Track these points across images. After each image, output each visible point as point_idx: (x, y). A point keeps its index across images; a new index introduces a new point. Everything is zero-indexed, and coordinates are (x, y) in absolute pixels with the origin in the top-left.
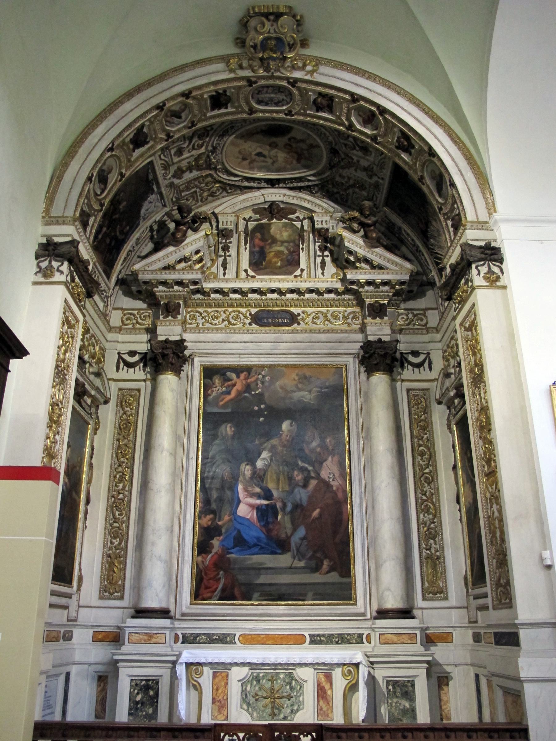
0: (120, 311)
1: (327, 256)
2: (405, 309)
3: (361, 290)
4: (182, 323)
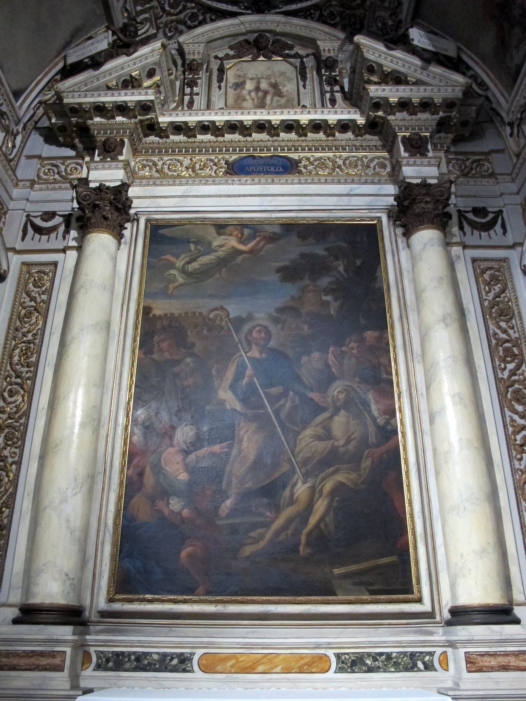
0: (36, 160)
1: (337, 92)
2: (456, 153)
3: (390, 118)
4: (125, 165)
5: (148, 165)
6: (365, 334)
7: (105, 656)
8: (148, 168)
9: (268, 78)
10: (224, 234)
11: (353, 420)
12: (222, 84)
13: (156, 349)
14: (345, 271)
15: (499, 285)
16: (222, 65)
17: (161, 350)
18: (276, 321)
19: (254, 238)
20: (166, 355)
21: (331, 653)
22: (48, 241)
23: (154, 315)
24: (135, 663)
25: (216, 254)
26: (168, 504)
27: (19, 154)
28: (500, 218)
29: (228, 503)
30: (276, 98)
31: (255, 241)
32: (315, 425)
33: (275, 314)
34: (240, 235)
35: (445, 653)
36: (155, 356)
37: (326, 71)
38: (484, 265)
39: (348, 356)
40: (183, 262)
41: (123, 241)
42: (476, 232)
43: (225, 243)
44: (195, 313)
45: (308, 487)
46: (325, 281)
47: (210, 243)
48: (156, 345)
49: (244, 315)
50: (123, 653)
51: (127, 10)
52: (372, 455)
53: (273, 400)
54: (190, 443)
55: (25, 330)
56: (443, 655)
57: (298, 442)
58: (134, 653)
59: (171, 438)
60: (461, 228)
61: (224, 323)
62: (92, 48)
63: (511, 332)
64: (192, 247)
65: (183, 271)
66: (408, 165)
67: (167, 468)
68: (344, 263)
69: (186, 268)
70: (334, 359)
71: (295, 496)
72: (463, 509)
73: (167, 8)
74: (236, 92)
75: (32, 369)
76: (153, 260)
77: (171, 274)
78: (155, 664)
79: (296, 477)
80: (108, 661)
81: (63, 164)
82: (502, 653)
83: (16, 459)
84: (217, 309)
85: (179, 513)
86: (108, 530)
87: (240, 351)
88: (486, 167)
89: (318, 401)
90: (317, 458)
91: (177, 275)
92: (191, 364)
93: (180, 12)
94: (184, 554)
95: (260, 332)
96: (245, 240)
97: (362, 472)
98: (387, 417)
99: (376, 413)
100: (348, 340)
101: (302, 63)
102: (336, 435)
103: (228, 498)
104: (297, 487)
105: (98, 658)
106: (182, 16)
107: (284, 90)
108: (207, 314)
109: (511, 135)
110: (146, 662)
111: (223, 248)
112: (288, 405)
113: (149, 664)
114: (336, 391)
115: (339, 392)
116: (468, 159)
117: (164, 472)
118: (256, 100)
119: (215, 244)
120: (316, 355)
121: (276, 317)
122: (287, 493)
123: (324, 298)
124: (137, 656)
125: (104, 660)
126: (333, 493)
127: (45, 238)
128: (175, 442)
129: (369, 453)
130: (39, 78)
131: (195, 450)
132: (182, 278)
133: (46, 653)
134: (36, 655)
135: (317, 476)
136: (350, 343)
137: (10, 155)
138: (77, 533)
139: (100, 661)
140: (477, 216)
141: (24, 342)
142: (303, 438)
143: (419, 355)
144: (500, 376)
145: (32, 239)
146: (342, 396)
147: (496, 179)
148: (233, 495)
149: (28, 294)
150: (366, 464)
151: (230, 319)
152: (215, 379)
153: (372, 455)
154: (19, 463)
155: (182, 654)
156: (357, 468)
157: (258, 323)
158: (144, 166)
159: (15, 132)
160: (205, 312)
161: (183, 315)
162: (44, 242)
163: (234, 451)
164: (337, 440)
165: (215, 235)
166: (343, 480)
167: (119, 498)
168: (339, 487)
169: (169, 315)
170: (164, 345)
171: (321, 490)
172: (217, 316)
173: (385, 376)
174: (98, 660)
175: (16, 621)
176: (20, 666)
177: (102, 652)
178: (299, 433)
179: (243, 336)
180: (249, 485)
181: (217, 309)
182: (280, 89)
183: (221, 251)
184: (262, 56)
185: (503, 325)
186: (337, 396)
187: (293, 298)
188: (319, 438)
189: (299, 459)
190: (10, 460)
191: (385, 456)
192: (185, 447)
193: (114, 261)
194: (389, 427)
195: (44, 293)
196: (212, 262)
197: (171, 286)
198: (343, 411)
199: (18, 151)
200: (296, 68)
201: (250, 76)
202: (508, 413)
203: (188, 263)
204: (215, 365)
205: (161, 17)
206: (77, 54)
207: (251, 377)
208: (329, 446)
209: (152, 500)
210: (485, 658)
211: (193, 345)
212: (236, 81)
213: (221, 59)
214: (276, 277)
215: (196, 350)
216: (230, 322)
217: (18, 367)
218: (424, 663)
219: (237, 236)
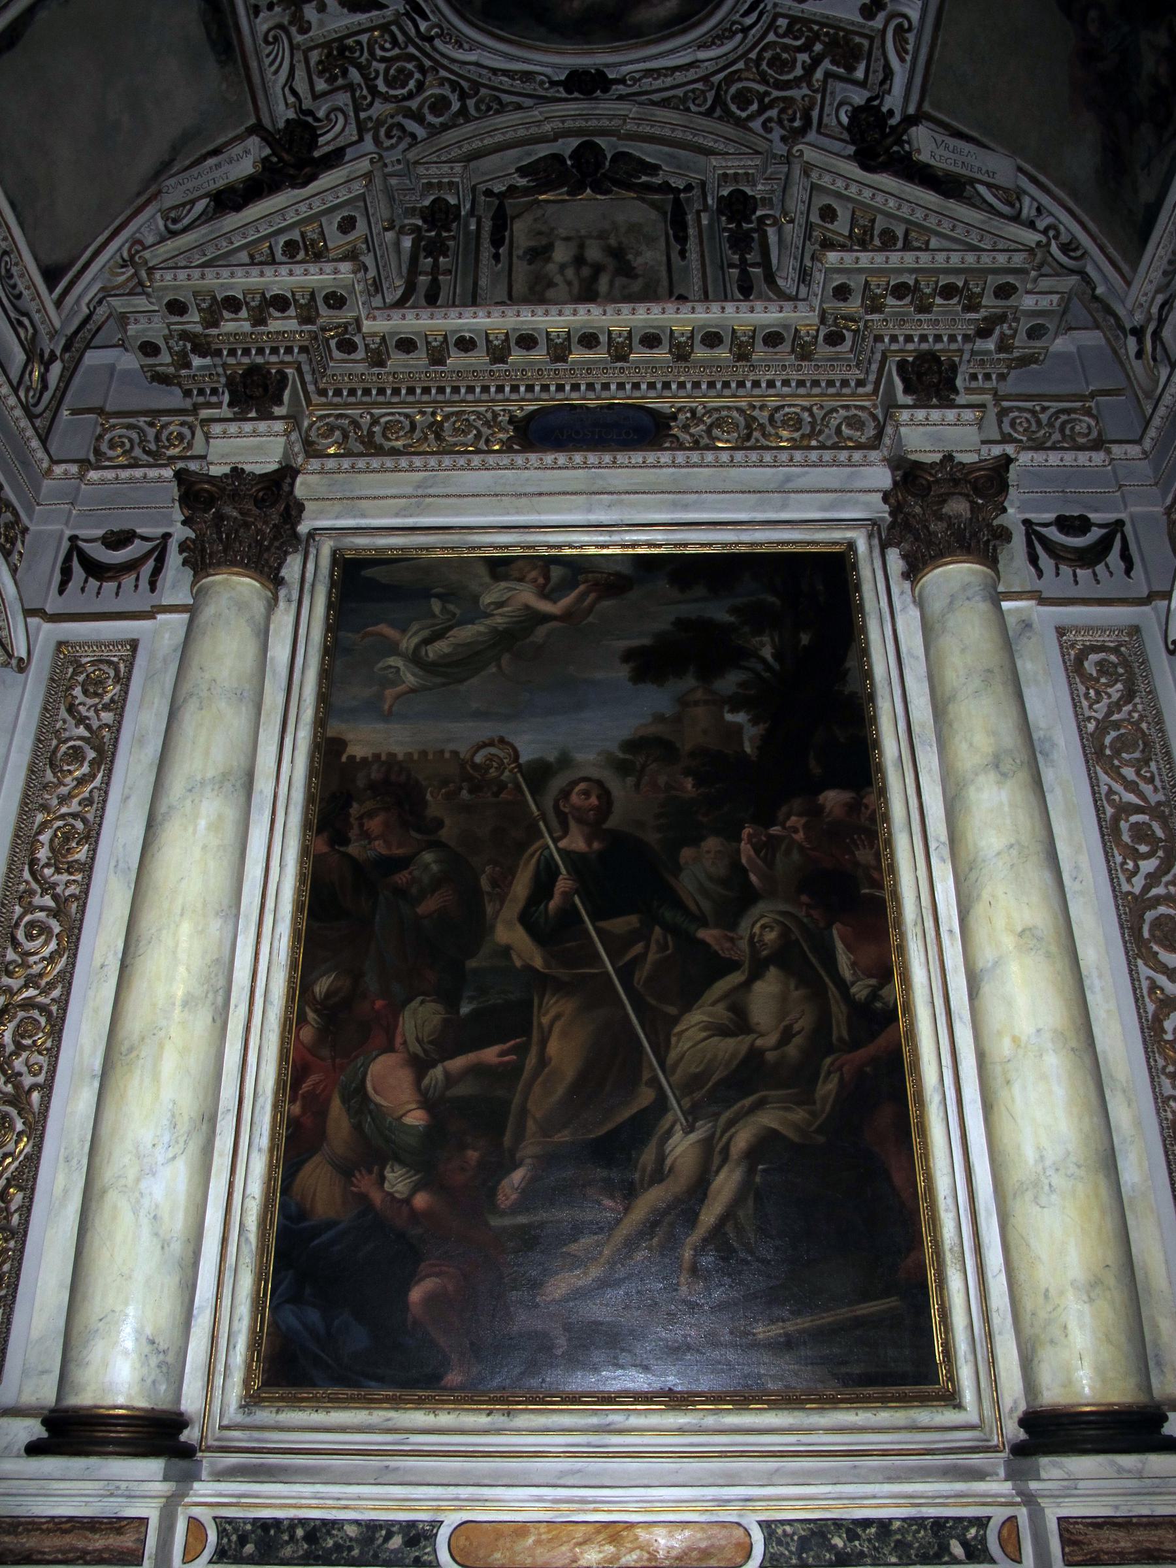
1: (753, 265)
5: (338, 427)
6: (821, 798)
7: (236, 1530)
8: (337, 433)
9: (602, 236)
10: (506, 578)
11: (797, 989)
12: (501, 251)
13: (353, 834)
14: (776, 656)
15: (1119, 686)
16: (501, 209)
17: (366, 835)
18: (622, 768)
19: (575, 586)
20: (379, 847)
21: (751, 1521)
22: (117, 594)
23: (352, 758)
24: (306, 1546)
25: (488, 622)
26: (382, 1179)
28: (1119, 536)
29: (518, 1176)
30: (620, 281)
31: (574, 594)
32: (710, 1002)
33: (621, 755)
34: (541, 581)
35: (1012, 1519)
36: (353, 849)
37: (729, 221)
38: (1083, 639)
39: (783, 847)
40: (416, 640)
41: (282, 593)
42: (1065, 569)
43: (509, 599)
44: (442, 752)
45: (698, 1141)
46: (729, 682)
47: (476, 599)
49: (551, 757)
50: (277, 1522)
51: (294, 93)
52: (840, 1069)
53: (616, 948)
54: (430, 1042)
55: (64, 790)
56: (1008, 1524)
57: (674, 1040)
58: (303, 1522)
59: (390, 1031)
60: (1033, 560)
61: (507, 773)
62: (217, 174)
63: (1147, 789)
64: (436, 606)
65: (416, 659)
66: (912, 422)
67: (378, 1099)
68: (773, 640)
69: (423, 653)
70: (752, 853)
71: (668, 1162)
72: (1047, 1188)
73: (382, 88)
74: (533, 267)
75: (78, 877)
76: (350, 635)
77: (390, 667)
78: (350, 1549)
79: (670, 1117)
80: (243, 1540)
81: (151, 425)
82: (1145, 1520)
83: (41, 1079)
84: (491, 744)
85: (407, 1201)
86: (247, 1239)
87: (542, 837)
88: (1084, 425)
89: (717, 948)
90: (716, 1077)
91: (402, 668)
92: (435, 868)
93: (410, 96)
94: (416, 1294)
95: (587, 794)
96: (553, 590)
97: (818, 1106)
98: (873, 981)
99: (847, 973)
100: (784, 809)
101: (677, 203)
102: (758, 1024)
103: (515, 1167)
104: (670, 1141)
105: (222, 1533)
106: (414, 104)
107: (638, 262)
108: (468, 757)
109: (1139, 354)
110: (330, 1543)
111: (506, 609)
112: (652, 957)
113: (338, 1547)
114: (758, 925)
115: (763, 927)
116: (1044, 409)
117: (372, 1106)
118: (576, 283)
119: (487, 599)
120: (712, 843)
121: (624, 760)
122: (648, 1156)
123: (729, 717)
124: (308, 1529)
125: (234, 1538)
126: (753, 1155)
127: (110, 586)
128: (398, 1040)
129: (832, 1064)
130: (101, 239)
131: (443, 1060)
132: (414, 675)
133: (102, 1523)
134: (79, 1528)
135: (717, 1115)
136: (788, 818)
137: (36, 405)
138: (177, 1247)
139: (225, 1540)
140: (1067, 534)
141: (62, 817)
142: (687, 1030)
143: (944, 844)
144: (1126, 887)
145: (83, 589)
146: (771, 936)
147: (1108, 451)
148: (528, 1161)
149: (71, 709)
150: (827, 1088)
151: (519, 766)
152: (486, 899)
153: (840, 1069)
154: (47, 1088)
155: (412, 1524)
156: (806, 1099)
157: (582, 774)
158: (331, 429)
160: (464, 750)
161: (416, 757)
162: (107, 596)
163: (532, 1060)
164: (762, 1035)
165: (487, 579)
166: (774, 1125)
167: (271, 1167)
168: (767, 1142)
169: (383, 757)
170: (375, 825)
171: (726, 1150)
172: (491, 758)
173: (867, 891)
174: (220, 1538)
175: (34, 1449)
176: (44, 1553)
177: (230, 1521)
178: (676, 1020)
179: (549, 803)
180: (564, 1136)
181: (491, 744)
182: (629, 262)
183: (501, 615)
184: (588, 190)
185: (1129, 773)
186: (761, 935)
187: (659, 718)
188: (723, 1032)
189: (675, 1078)
190: (28, 1081)
191: (868, 1069)
192: (422, 1054)
193: (262, 636)
194: (879, 1005)
195: (106, 708)
196: (480, 639)
197: (390, 693)
198: (773, 972)
199: (54, 395)
200: (665, 213)
201: (563, 232)
202: (1144, 971)
203: (427, 642)
204: (488, 869)
205: (371, 105)
206: (184, 188)
207: (567, 896)
208: (744, 1049)
209: (346, 1171)
210: (1106, 1533)
211: (440, 824)
212: (533, 243)
213: (501, 196)
214: (623, 672)
215: (444, 834)
216: (520, 771)
217: (48, 872)
218: (965, 1544)
219: (535, 580)
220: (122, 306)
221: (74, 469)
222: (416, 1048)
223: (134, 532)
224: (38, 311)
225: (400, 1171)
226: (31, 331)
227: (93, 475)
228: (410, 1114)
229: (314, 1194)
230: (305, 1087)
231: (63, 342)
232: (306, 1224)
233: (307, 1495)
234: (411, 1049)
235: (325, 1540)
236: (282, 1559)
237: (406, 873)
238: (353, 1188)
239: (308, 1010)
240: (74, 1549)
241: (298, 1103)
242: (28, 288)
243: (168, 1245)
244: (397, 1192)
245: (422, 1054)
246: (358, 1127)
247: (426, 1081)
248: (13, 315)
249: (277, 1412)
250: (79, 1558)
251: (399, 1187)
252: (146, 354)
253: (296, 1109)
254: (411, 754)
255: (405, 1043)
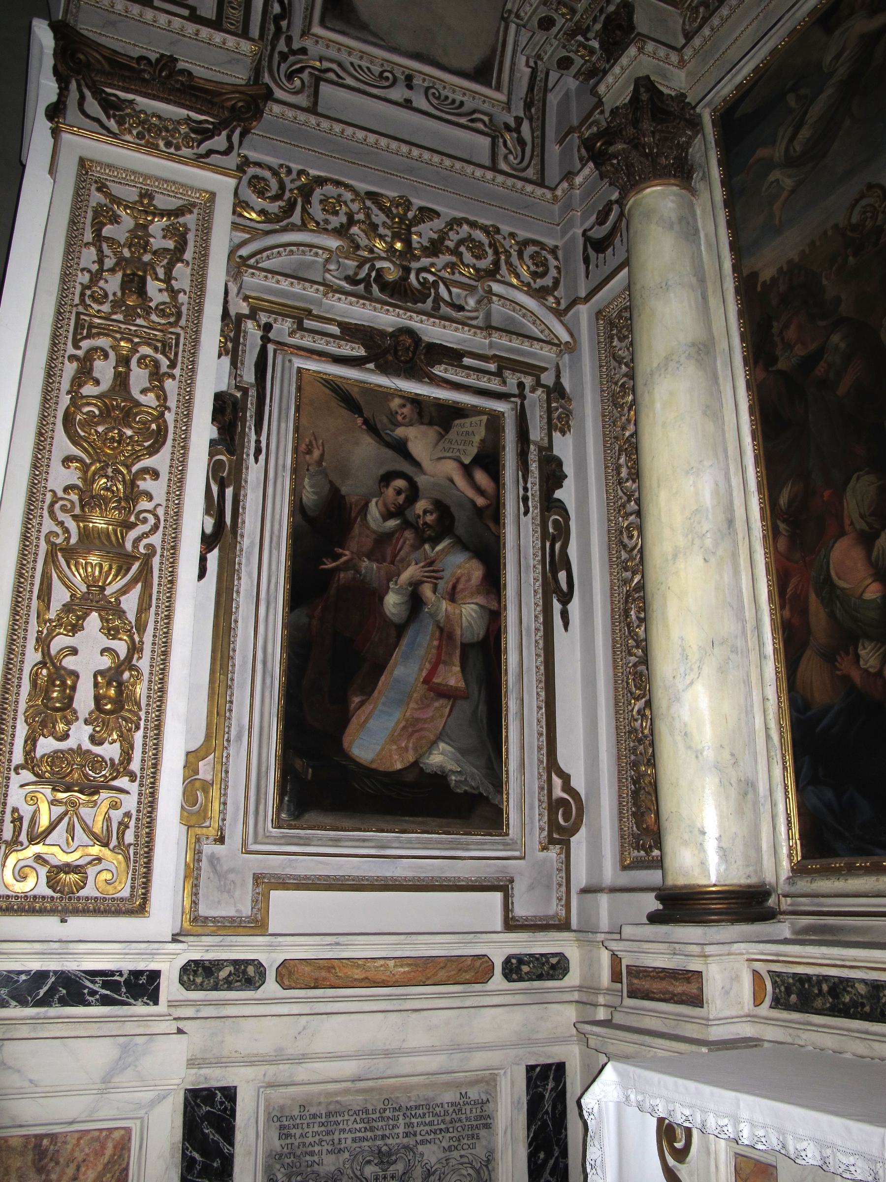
7: (783, 982)
20: (800, 351)
22: (614, 255)
24: (831, 1000)
26: (857, 657)
27: (537, 151)
48: (777, 339)
50: (808, 978)
54: (871, 515)
58: (826, 978)
65: (790, 162)
77: (772, 183)
78: (863, 1005)
105: (774, 983)
110: (847, 999)
113: (855, 1004)
117: (839, 592)
124: (831, 985)
125: (783, 988)
128: (847, 522)
132: (789, 177)
133: (679, 974)
134: (668, 977)
139: (777, 991)
145: (597, 266)
159: (513, 124)
170: (791, 334)
174: (774, 989)
175: (654, 918)
176: (654, 993)
192: (866, 528)
209: (829, 657)
220: (533, 50)
221: (565, 185)
222: (861, 525)
223: (611, 201)
224: (484, 102)
225: (869, 646)
226: (486, 119)
227: (578, 180)
228: (868, 590)
229: (811, 683)
230: (789, 591)
231: (522, 104)
232: (809, 713)
233: (817, 955)
234: (858, 527)
235: (843, 996)
236: (816, 1009)
237: (822, 363)
238: (838, 673)
239: (778, 522)
240: (668, 992)
241: (787, 607)
242: (464, 94)
243: (701, 754)
244: (870, 667)
245: (866, 528)
246: (831, 615)
247: (875, 553)
248: (463, 121)
249: (811, 882)
250: (672, 998)
251: (872, 662)
252: (567, 68)
253: (787, 613)
254: (803, 251)
255: (852, 523)
